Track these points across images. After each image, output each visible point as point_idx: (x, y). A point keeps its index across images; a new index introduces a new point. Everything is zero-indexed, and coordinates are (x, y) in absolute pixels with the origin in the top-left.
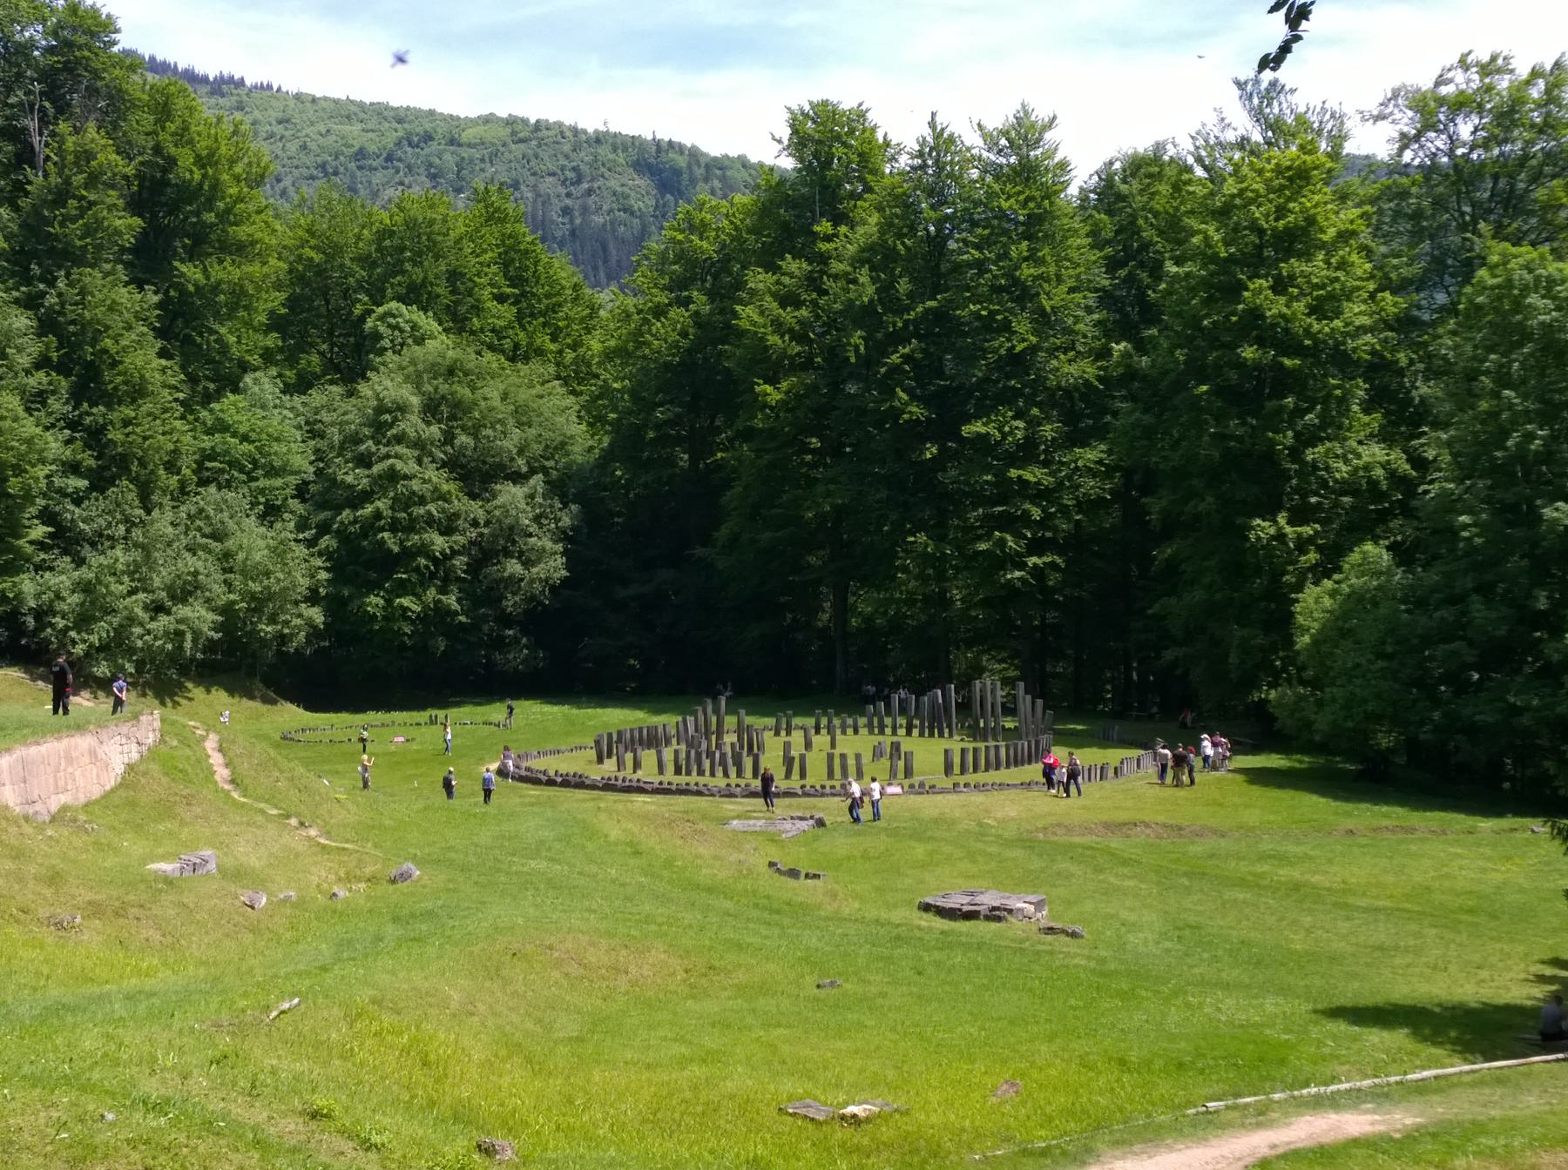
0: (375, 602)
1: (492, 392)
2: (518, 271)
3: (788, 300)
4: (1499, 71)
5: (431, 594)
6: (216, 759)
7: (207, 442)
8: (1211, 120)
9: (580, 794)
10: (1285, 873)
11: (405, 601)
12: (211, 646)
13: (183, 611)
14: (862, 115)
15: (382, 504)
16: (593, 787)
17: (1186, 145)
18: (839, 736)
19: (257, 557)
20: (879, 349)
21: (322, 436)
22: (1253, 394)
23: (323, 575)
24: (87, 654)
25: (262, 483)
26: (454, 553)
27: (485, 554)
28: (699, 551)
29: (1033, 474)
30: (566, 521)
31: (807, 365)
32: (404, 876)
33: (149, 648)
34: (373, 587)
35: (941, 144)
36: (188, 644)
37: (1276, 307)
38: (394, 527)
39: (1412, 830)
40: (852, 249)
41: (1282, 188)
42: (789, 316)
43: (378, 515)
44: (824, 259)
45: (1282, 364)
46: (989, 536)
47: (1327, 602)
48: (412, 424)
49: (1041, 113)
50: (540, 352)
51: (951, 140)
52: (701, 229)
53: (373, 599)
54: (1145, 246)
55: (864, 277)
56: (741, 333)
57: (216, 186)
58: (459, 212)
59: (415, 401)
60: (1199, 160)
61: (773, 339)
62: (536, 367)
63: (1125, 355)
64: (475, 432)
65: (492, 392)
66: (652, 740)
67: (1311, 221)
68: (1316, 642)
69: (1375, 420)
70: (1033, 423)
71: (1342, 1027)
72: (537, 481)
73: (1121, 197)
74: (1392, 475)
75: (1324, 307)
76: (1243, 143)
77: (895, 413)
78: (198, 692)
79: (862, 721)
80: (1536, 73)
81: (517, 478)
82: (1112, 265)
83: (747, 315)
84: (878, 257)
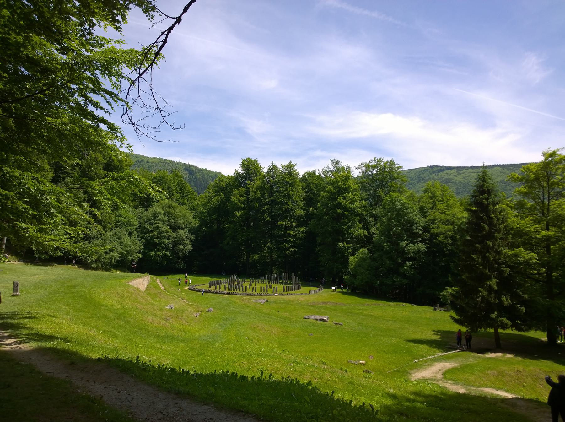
0: (153, 253)
1: (178, 211)
2: (181, 187)
3: (241, 196)
4: (381, 161)
5: (164, 252)
6: (160, 285)
7: (117, 219)
8: (326, 167)
9: (211, 294)
10: (367, 313)
11: (159, 253)
12: (118, 261)
13: (112, 254)
14: (257, 161)
15: (155, 233)
16: (213, 293)
17: (321, 170)
18: (257, 284)
19: (129, 243)
20: (261, 206)
21: (140, 219)
22: (338, 218)
23: (142, 247)
24: (91, 262)
25: (129, 228)
26: (169, 243)
27: (175, 244)
28: (220, 245)
29: (291, 232)
30: (192, 238)
31: (245, 208)
32: (211, 311)
33: (104, 262)
34: (152, 250)
35: (274, 167)
36: (113, 261)
37: (344, 202)
38: (158, 238)
39: (379, 304)
40: (255, 186)
41: (343, 180)
42: (241, 199)
43: (154, 235)
44: (248, 188)
45: (345, 214)
46: (283, 244)
47: (356, 259)
48: (162, 217)
49: (293, 163)
50: (185, 204)
51: (276, 167)
52: (222, 181)
53: (152, 253)
54: (312, 190)
55: (258, 192)
56: (231, 202)
57: (122, 166)
58: (170, 176)
59: (163, 212)
60: (323, 174)
61: (238, 203)
62: (185, 207)
63: (313, 210)
64: (174, 219)
65: (178, 211)
66: (219, 283)
67: (350, 186)
68: (354, 268)
69: (360, 225)
70: (292, 222)
71: (411, 344)
72: (186, 229)
73: (307, 180)
74: (365, 235)
75: (352, 203)
76: (331, 171)
77: (264, 219)
78: (114, 271)
79: (260, 280)
80: (387, 162)
81: (182, 229)
82: (306, 193)
83: (234, 198)
84: (261, 188)
